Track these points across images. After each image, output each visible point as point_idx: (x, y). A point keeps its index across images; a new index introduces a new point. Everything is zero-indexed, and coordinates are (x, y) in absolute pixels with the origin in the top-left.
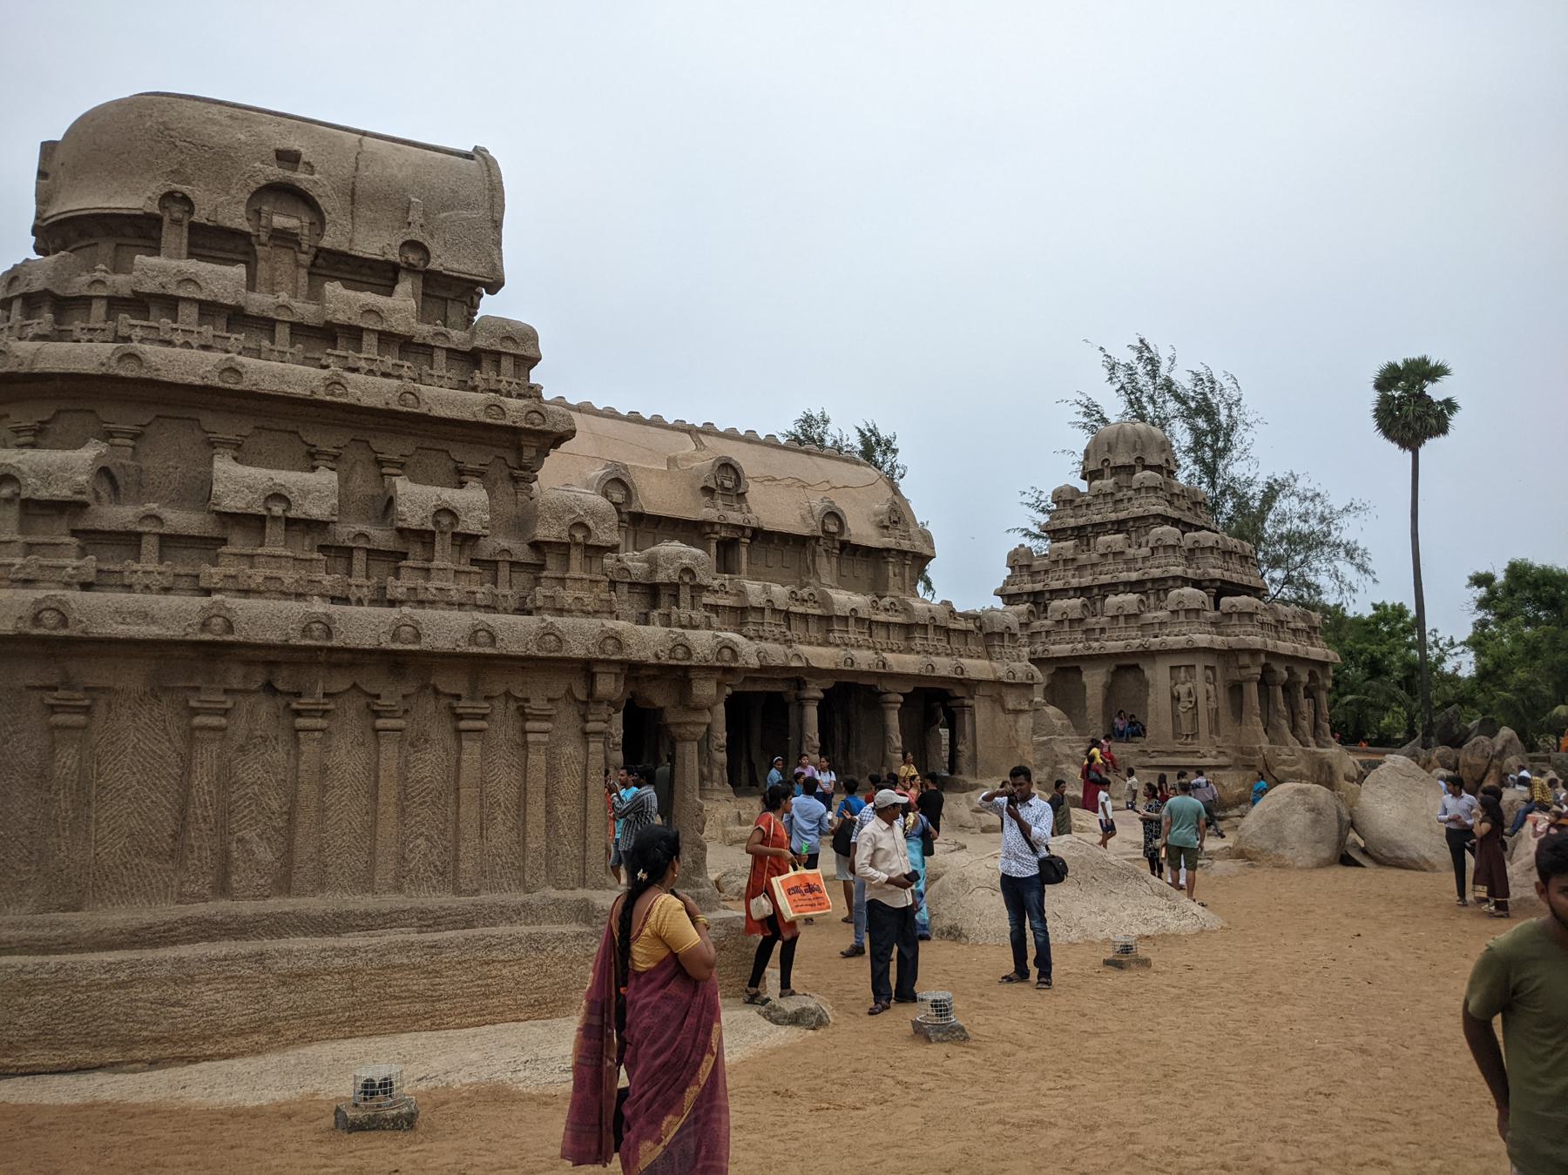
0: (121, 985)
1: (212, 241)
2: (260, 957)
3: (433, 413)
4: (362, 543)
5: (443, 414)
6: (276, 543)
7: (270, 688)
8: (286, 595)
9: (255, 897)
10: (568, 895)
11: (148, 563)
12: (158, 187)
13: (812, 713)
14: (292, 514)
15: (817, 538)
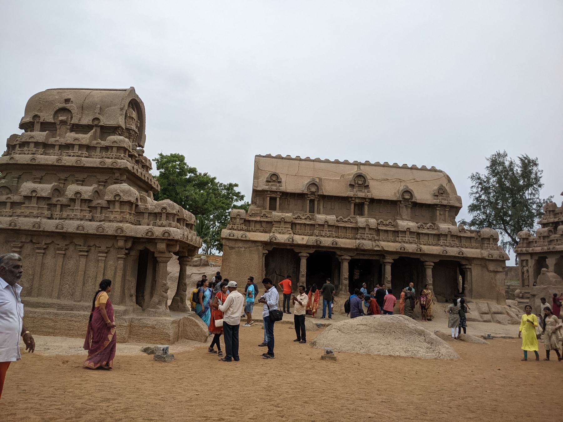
1: (45, 126)
3: (85, 166)
4: (59, 203)
6: (34, 203)
8: (35, 217)
13: (388, 268)
15: (400, 201)
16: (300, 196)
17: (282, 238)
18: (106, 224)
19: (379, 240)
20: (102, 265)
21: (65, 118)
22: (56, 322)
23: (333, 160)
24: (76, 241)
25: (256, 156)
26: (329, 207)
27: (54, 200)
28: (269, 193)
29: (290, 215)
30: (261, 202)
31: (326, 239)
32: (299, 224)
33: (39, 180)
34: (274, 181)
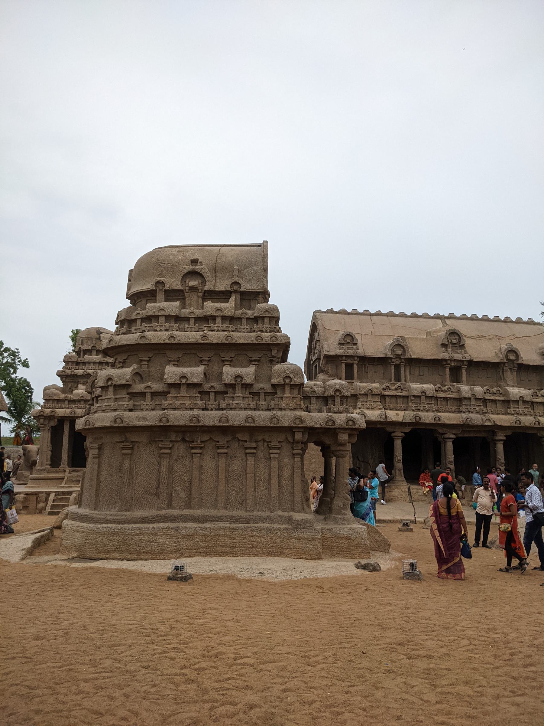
0: (137, 535)
1: (171, 295)
2: (177, 528)
4: (212, 390)
5: (241, 342)
6: (184, 392)
7: (184, 440)
8: (187, 409)
9: (180, 509)
10: (286, 514)
11: (148, 402)
12: (154, 280)
13: (500, 447)
14: (188, 382)
16: (382, 361)
18: (279, 414)
19: (487, 413)
20: (275, 464)
21: (196, 283)
22: (234, 538)
24: (240, 436)
25: (316, 312)
26: (417, 372)
27: (206, 387)
28: (344, 358)
29: (377, 385)
31: (426, 414)
32: (388, 396)
33: (177, 363)
34: (349, 343)
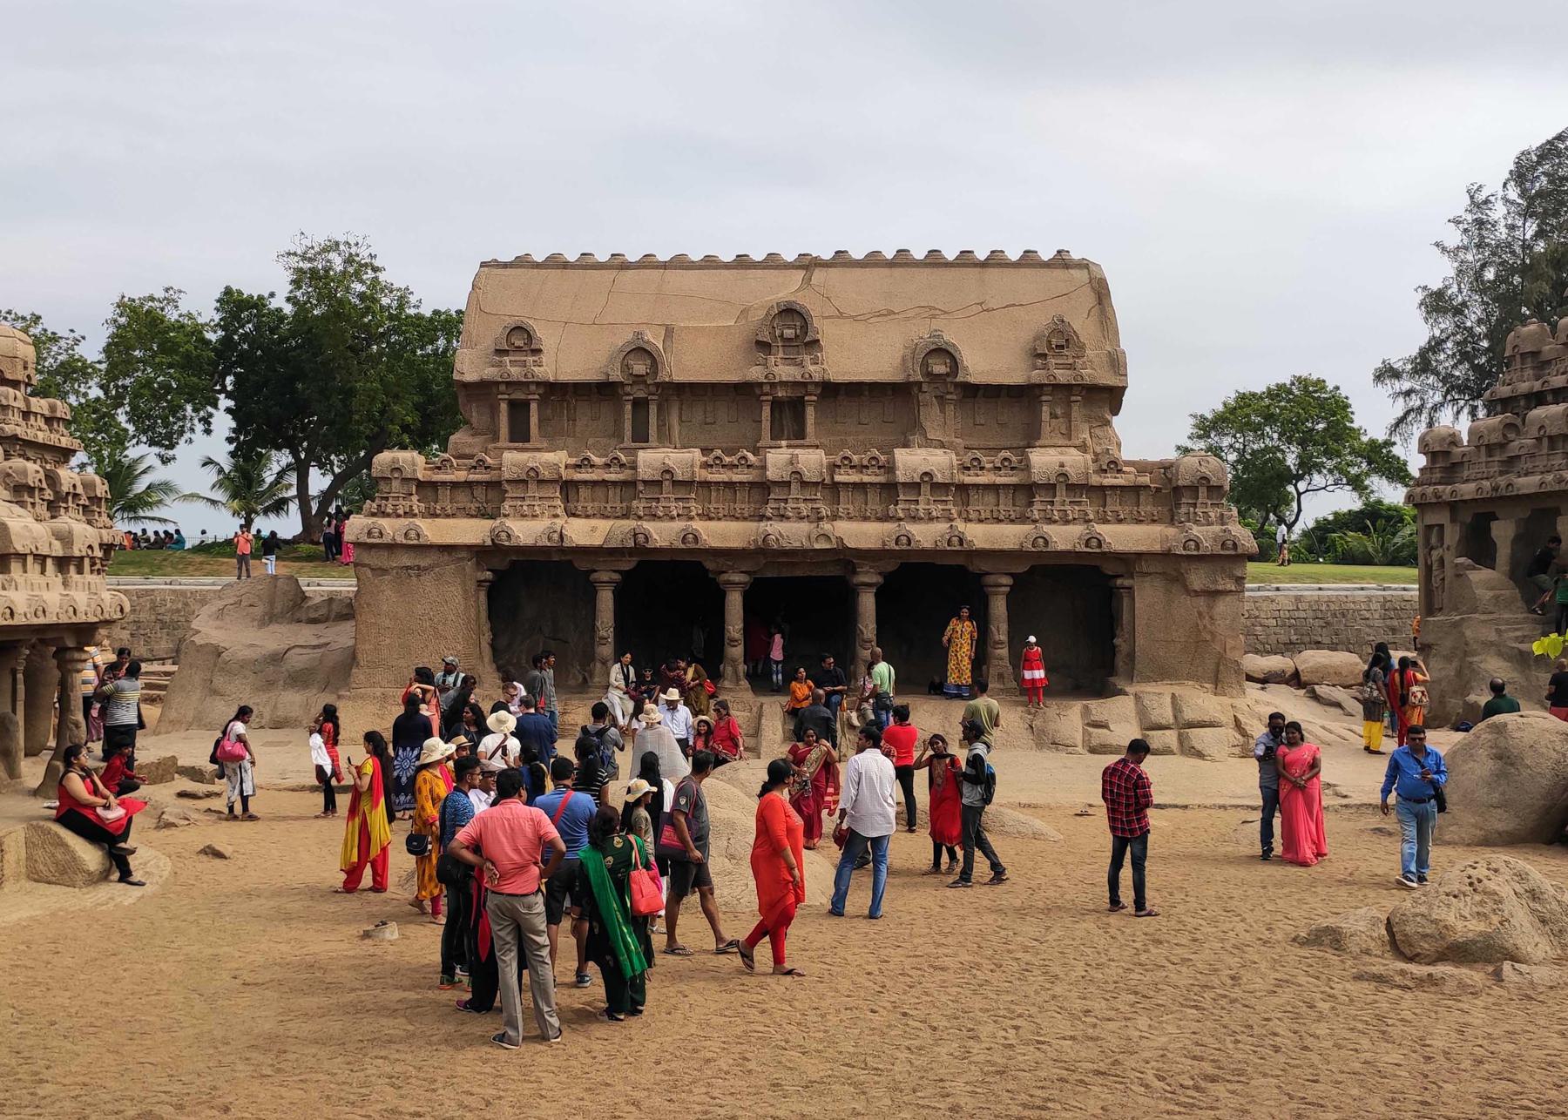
13: (867, 603)
16: (602, 392)
17: (525, 530)
23: (727, 257)
25: (483, 265)
28: (502, 388)
30: (486, 418)
32: (585, 482)
